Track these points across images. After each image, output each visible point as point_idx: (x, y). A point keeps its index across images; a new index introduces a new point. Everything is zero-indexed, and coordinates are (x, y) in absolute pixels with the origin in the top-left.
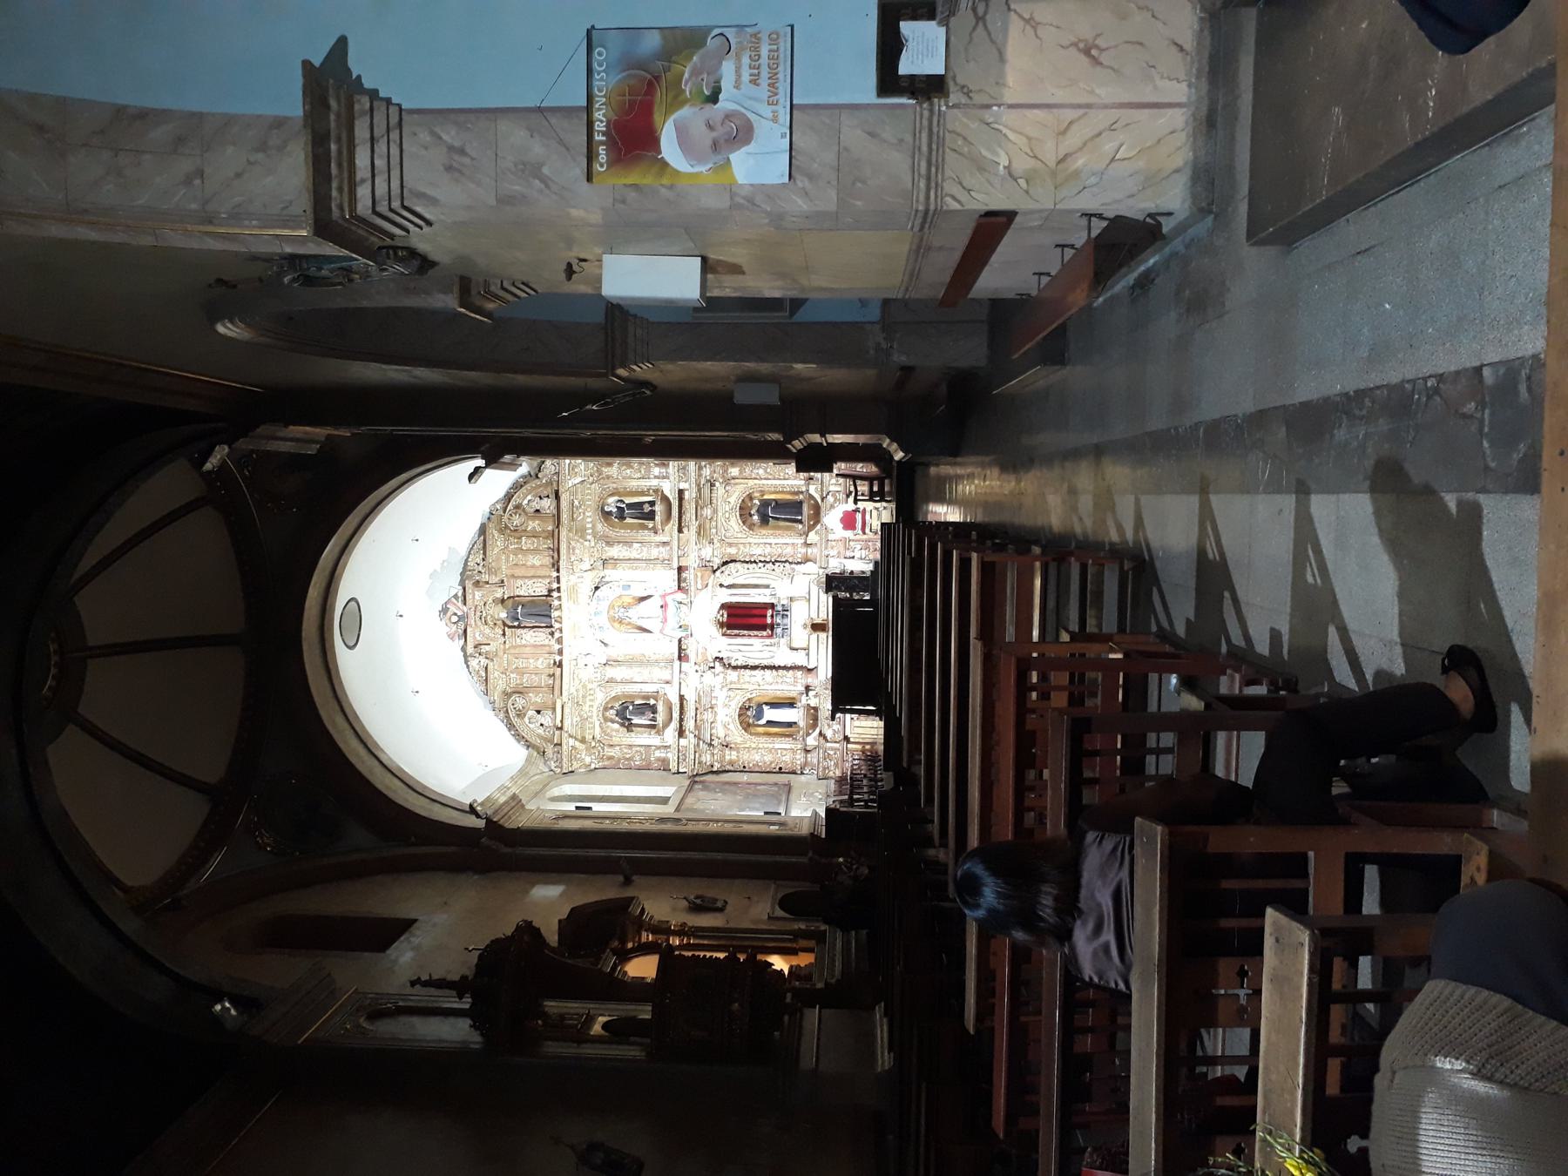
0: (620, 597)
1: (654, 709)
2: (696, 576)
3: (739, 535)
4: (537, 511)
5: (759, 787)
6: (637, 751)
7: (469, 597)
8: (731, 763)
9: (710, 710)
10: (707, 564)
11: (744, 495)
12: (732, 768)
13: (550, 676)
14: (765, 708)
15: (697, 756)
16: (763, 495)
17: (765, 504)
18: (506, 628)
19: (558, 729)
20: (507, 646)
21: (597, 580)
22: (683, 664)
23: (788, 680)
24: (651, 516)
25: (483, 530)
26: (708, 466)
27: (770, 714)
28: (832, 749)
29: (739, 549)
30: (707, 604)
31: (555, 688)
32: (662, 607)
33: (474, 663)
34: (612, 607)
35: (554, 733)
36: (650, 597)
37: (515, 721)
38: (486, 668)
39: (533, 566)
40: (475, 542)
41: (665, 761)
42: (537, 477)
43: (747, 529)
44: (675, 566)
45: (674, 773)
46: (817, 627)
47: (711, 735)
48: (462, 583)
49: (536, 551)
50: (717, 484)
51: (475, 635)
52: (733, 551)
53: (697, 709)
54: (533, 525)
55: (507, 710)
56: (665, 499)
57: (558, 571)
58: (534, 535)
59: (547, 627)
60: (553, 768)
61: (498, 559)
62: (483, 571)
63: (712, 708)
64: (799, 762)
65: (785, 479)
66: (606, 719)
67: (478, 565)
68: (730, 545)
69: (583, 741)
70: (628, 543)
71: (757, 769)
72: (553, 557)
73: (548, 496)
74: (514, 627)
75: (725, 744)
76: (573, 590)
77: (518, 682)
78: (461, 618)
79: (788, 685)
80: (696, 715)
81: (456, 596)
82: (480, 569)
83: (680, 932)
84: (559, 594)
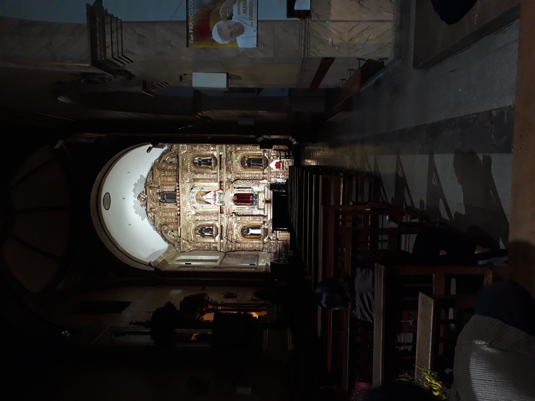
0: (200, 192)
1: (212, 230)
2: (226, 184)
3: (241, 171)
4: (171, 162)
5: (248, 256)
6: (206, 244)
7: (148, 192)
8: (239, 248)
9: (231, 230)
10: (230, 180)
11: (242, 157)
12: (239, 250)
13: (176, 219)
14: (250, 229)
15: (227, 245)
16: (248, 157)
18: (161, 203)
19: (179, 237)
20: (161, 209)
21: (192, 186)
22: (222, 215)
23: (258, 220)
24: (210, 164)
25: (152, 169)
26: (230, 147)
27: (252, 231)
28: (272, 243)
29: (241, 175)
30: (230, 194)
31: (178, 223)
32: (214, 195)
33: (150, 215)
34: (197, 195)
35: (178, 238)
36: (210, 192)
37: (164, 234)
38: (154, 216)
39: (170, 181)
40: (150, 173)
41: (216, 248)
42: (171, 151)
43: (243, 168)
44: (219, 181)
45: (219, 252)
46: (267, 202)
47: (232, 238)
48: (145, 187)
49: (170, 176)
50: (233, 153)
51: (150, 205)
52: (238, 176)
53: (227, 230)
54: (170, 167)
55: (161, 231)
56: (215, 158)
57: (178, 183)
58: (170, 171)
59: (175, 202)
60: (177, 250)
61: (158, 179)
64: (261, 247)
65: (256, 151)
66: (196, 234)
67: (151, 181)
68: (238, 174)
69: (188, 241)
70: (203, 173)
71: (247, 250)
72: (177, 178)
73: (174, 157)
74: (163, 202)
75: (236, 241)
76: (184, 190)
77: (165, 221)
78: (145, 199)
79: (257, 221)
80: (226, 232)
81: (143, 192)
83: (222, 305)
84: (178, 191)
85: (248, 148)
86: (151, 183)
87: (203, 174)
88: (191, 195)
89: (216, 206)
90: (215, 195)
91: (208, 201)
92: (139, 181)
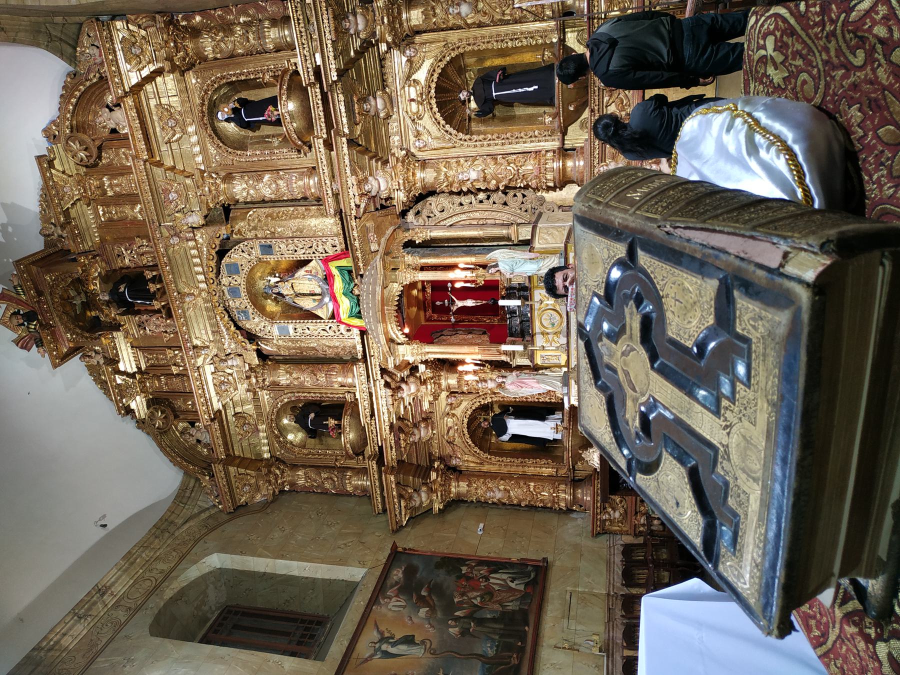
4: (114, 131)
8: (458, 494)
17: (485, 79)
21: (218, 242)
29: (438, 171)
43: (454, 132)
62: (65, 235)
63: (425, 420)
65: (516, 22)
82: (60, 232)
85: (464, 9)
86: (61, 236)
87: (260, 179)
88: (225, 281)
89: (342, 327)
90: (328, 279)
91: (307, 304)
92: (10, 229)
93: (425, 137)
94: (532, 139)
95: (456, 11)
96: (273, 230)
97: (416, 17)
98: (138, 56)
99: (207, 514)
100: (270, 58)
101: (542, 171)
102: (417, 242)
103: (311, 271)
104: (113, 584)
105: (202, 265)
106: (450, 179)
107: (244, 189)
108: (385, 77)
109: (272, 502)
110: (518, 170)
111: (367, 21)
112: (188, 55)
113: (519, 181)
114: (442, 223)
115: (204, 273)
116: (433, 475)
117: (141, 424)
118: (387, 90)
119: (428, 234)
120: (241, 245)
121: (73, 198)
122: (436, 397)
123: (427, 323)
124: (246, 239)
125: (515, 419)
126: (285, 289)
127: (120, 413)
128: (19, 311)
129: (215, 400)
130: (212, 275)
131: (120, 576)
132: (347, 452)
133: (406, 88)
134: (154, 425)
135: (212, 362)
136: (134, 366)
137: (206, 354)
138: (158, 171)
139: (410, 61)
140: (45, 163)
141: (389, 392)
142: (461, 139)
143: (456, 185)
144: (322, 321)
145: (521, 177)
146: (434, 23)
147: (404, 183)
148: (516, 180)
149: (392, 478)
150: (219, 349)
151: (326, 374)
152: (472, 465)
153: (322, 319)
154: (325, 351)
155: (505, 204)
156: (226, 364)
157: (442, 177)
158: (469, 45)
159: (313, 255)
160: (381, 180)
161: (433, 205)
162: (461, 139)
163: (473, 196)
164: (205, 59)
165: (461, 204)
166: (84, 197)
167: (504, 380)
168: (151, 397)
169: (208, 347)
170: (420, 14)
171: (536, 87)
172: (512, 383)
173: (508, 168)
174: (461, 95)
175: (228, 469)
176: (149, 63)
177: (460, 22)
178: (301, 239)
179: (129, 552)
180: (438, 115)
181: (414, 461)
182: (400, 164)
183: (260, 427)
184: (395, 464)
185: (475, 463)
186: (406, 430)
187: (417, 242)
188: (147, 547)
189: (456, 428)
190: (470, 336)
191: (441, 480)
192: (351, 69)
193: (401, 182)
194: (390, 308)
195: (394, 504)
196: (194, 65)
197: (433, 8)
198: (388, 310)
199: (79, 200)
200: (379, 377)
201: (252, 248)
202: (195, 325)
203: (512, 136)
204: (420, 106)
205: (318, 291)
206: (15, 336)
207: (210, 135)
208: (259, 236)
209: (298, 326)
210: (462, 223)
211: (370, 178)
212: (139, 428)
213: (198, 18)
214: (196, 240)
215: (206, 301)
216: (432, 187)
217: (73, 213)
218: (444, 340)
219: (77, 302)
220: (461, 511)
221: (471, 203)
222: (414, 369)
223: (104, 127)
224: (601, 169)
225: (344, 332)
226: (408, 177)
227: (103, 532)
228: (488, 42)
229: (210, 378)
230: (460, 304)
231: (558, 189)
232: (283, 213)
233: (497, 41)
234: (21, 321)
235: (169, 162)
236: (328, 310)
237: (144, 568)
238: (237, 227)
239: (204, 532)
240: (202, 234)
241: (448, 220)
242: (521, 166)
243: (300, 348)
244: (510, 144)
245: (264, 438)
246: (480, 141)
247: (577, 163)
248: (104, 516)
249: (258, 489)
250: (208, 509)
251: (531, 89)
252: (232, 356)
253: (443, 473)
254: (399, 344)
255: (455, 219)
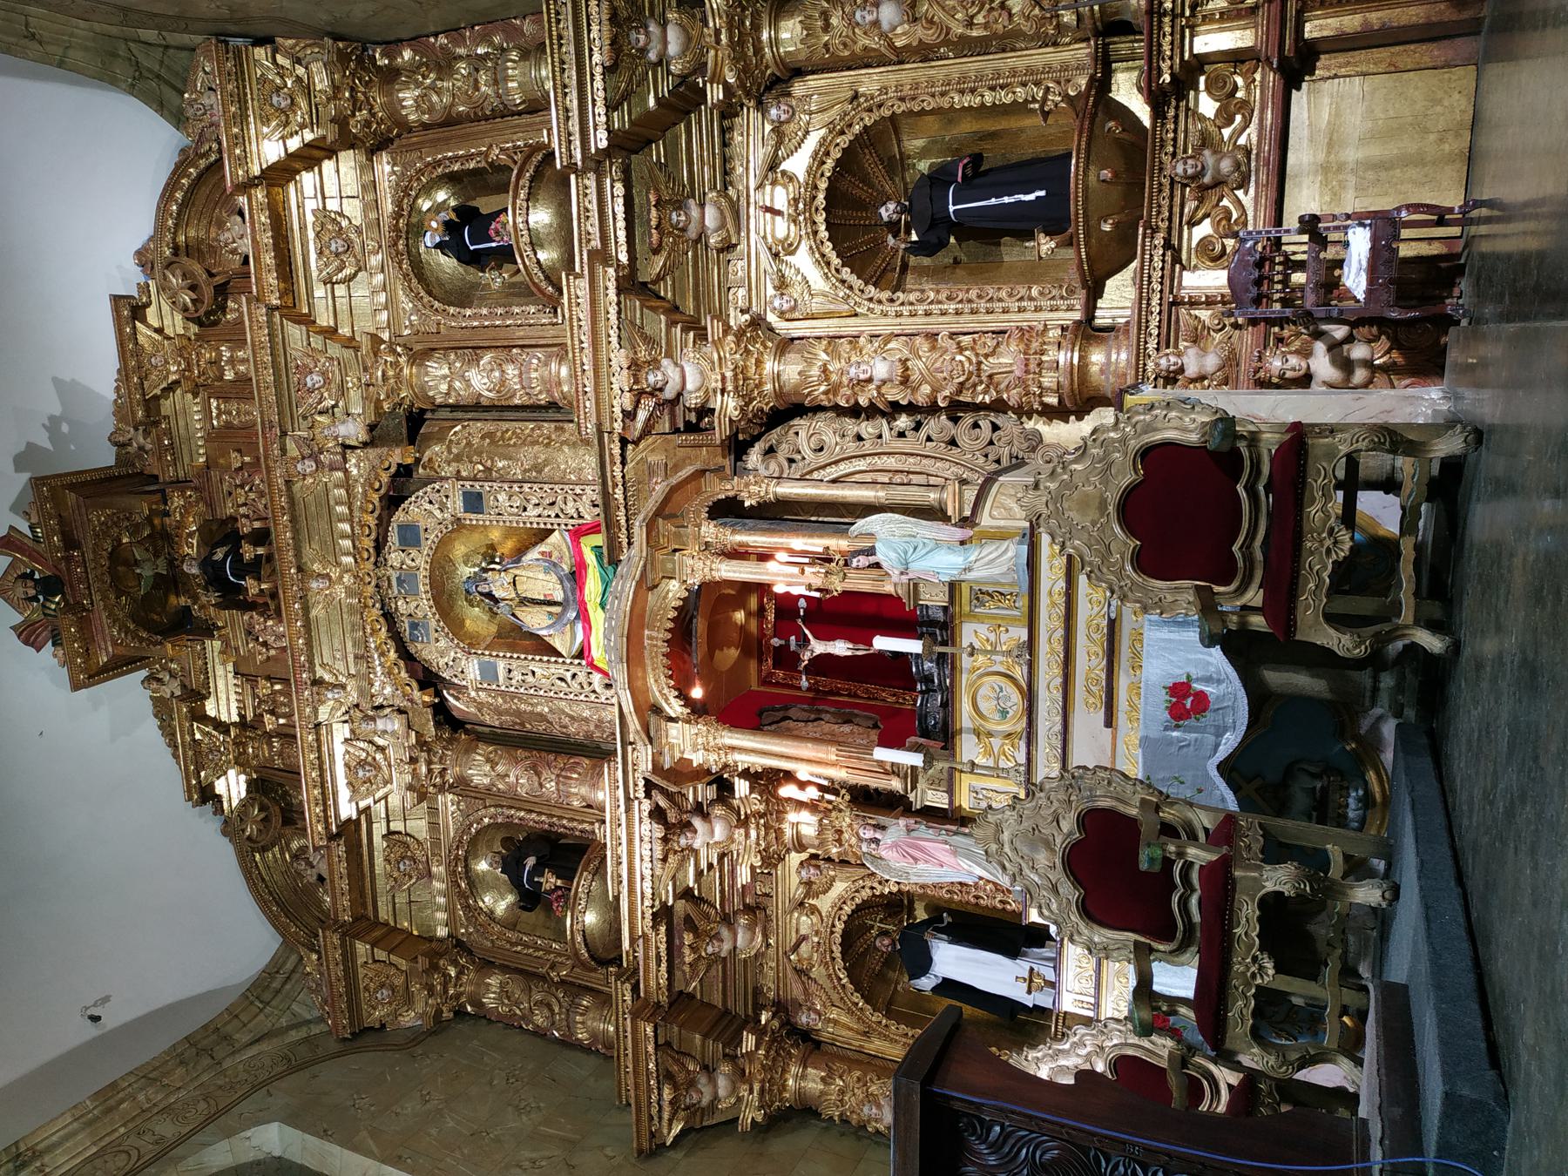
9: (743, 921)
11: (844, 141)
62: (149, 447)
63: (749, 909)
85: (888, 14)
86: (141, 448)
88: (395, 558)
91: (535, 620)
92: (65, 428)
93: (796, 291)
94: (1025, 304)
95: (869, 18)
96: (489, 463)
97: (789, 34)
98: (283, 111)
99: (303, 1033)
100: (518, 126)
101: (1033, 367)
102: (747, 504)
103: (550, 555)
104: (50, 1149)
105: (351, 521)
106: (834, 378)
107: (445, 377)
108: (728, 166)
109: (431, 1033)
110: (979, 363)
111: (689, 39)
112: (373, 115)
113: (980, 388)
114: (815, 475)
115: (353, 537)
116: (749, 1042)
117: (231, 827)
118: (731, 192)
119: (771, 489)
120: (429, 489)
121: (166, 378)
122: (771, 860)
123: (762, 689)
124: (442, 479)
125: (950, 942)
126: (500, 586)
127: (190, 799)
128: (33, 573)
129: (344, 793)
130: (368, 543)
131: (74, 1134)
132: (576, 954)
133: (768, 188)
134: (243, 831)
135: (346, 717)
136: (234, 712)
137: (336, 700)
138: (295, 332)
139: (778, 131)
140: (129, 311)
141: (659, 832)
142: (871, 300)
143: (846, 391)
144: (561, 660)
145: (984, 378)
146: (826, 45)
147: (736, 375)
148: (975, 386)
149: (649, 1030)
150: (361, 693)
151: (558, 776)
152: (844, 1033)
153: (559, 655)
154: (565, 727)
155: (953, 442)
156: (371, 726)
157: (815, 371)
158: (902, 99)
159: (558, 520)
160: (688, 369)
161: (802, 434)
162: (871, 300)
163: (884, 422)
164: (405, 127)
165: (859, 438)
166: (187, 378)
167: (878, 836)
168: (255, 776)
169: (343, 687)
170: (799, 27)
171: (1042, 193)
172: (895, 846)
173: (959, 358)
174: (882, 210)
175: (353, 946)
176: (302, 126)
177: (873, 42)
178: (536, 487)
179: (113, 1085)
180: (828, 248)
181: (717, 1000)
182: (730, 338)
183: (434, 869)
184: (664, 999)
185: (850, 1029)
186: (702, 925)
187: (747, 504)
188: (155, 1080)
189: (816, 939)
190: (846, 728)
191: (766, 1057)
192: (656, 142)
193: (729, 374)
194: (655, 634)
195: (650, 1090)
196: (391, 141)
197: (825, 16)
198: (651, 638)
199: (177, 382)
200: (641, 794)
201: (447, 497)
202: (324, 639)
203: (979, 297)
204: (792, 226)
205: (559, 596)
206: (18, 619)
207: (406, 276)
208: (464, 474)
209: (515, 664)
210: (857, 477)
211: (665, 362)
212: (225, 833)
213: (407, 54)
214: (346, 471)
215: (350, 592)
216: (797, 393)
217: (166, 406)
218: (788, 729)
219: (147, 572)
220: (804, 1138)
221: (880, 437)
222: (724, 788)
223: (234, 252)
224: (1163, 362)
225: (597, 686)
226: (745, 367)
227: (92, 1031)
228: (943, 94)
229: (339, 749)
230: (819, 647)
231: (1072, 418)
232: (514, 433)
233: (962, 92)
234: (32, 592)
235: (324, 320)
236: (573, 637)
237: (131, 1126)
238: (428, 454)
239: (280, 1069)
240: (359, 460)
241: (828, 470)
242: (986, 356)
243: (518, 713)
244: (973, 312)
245: (440, 893)
246: (911, 304)
247: (1114, 357)
248: (106, 999)
249: (409, 1000)
250: (309, 1022)
251: (1031, 197)
252: (388, 710)
253: (773, 1040)
254: (671, 719)
255: (844, 468)
